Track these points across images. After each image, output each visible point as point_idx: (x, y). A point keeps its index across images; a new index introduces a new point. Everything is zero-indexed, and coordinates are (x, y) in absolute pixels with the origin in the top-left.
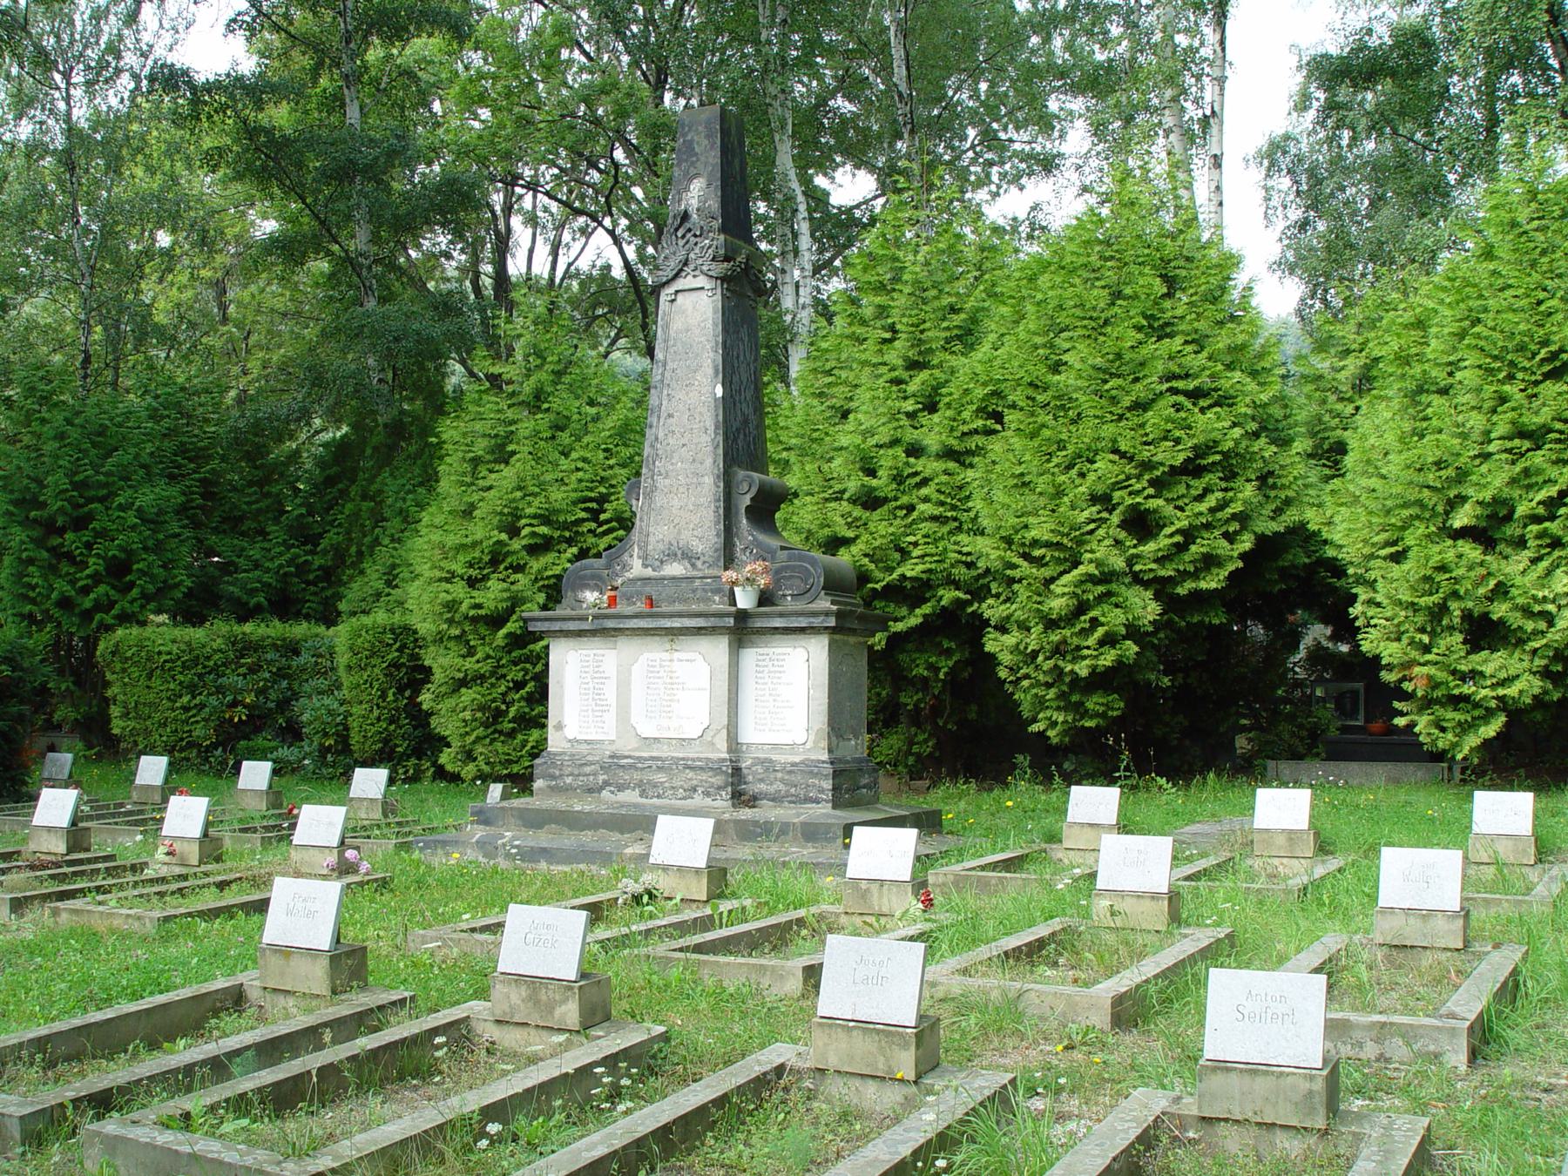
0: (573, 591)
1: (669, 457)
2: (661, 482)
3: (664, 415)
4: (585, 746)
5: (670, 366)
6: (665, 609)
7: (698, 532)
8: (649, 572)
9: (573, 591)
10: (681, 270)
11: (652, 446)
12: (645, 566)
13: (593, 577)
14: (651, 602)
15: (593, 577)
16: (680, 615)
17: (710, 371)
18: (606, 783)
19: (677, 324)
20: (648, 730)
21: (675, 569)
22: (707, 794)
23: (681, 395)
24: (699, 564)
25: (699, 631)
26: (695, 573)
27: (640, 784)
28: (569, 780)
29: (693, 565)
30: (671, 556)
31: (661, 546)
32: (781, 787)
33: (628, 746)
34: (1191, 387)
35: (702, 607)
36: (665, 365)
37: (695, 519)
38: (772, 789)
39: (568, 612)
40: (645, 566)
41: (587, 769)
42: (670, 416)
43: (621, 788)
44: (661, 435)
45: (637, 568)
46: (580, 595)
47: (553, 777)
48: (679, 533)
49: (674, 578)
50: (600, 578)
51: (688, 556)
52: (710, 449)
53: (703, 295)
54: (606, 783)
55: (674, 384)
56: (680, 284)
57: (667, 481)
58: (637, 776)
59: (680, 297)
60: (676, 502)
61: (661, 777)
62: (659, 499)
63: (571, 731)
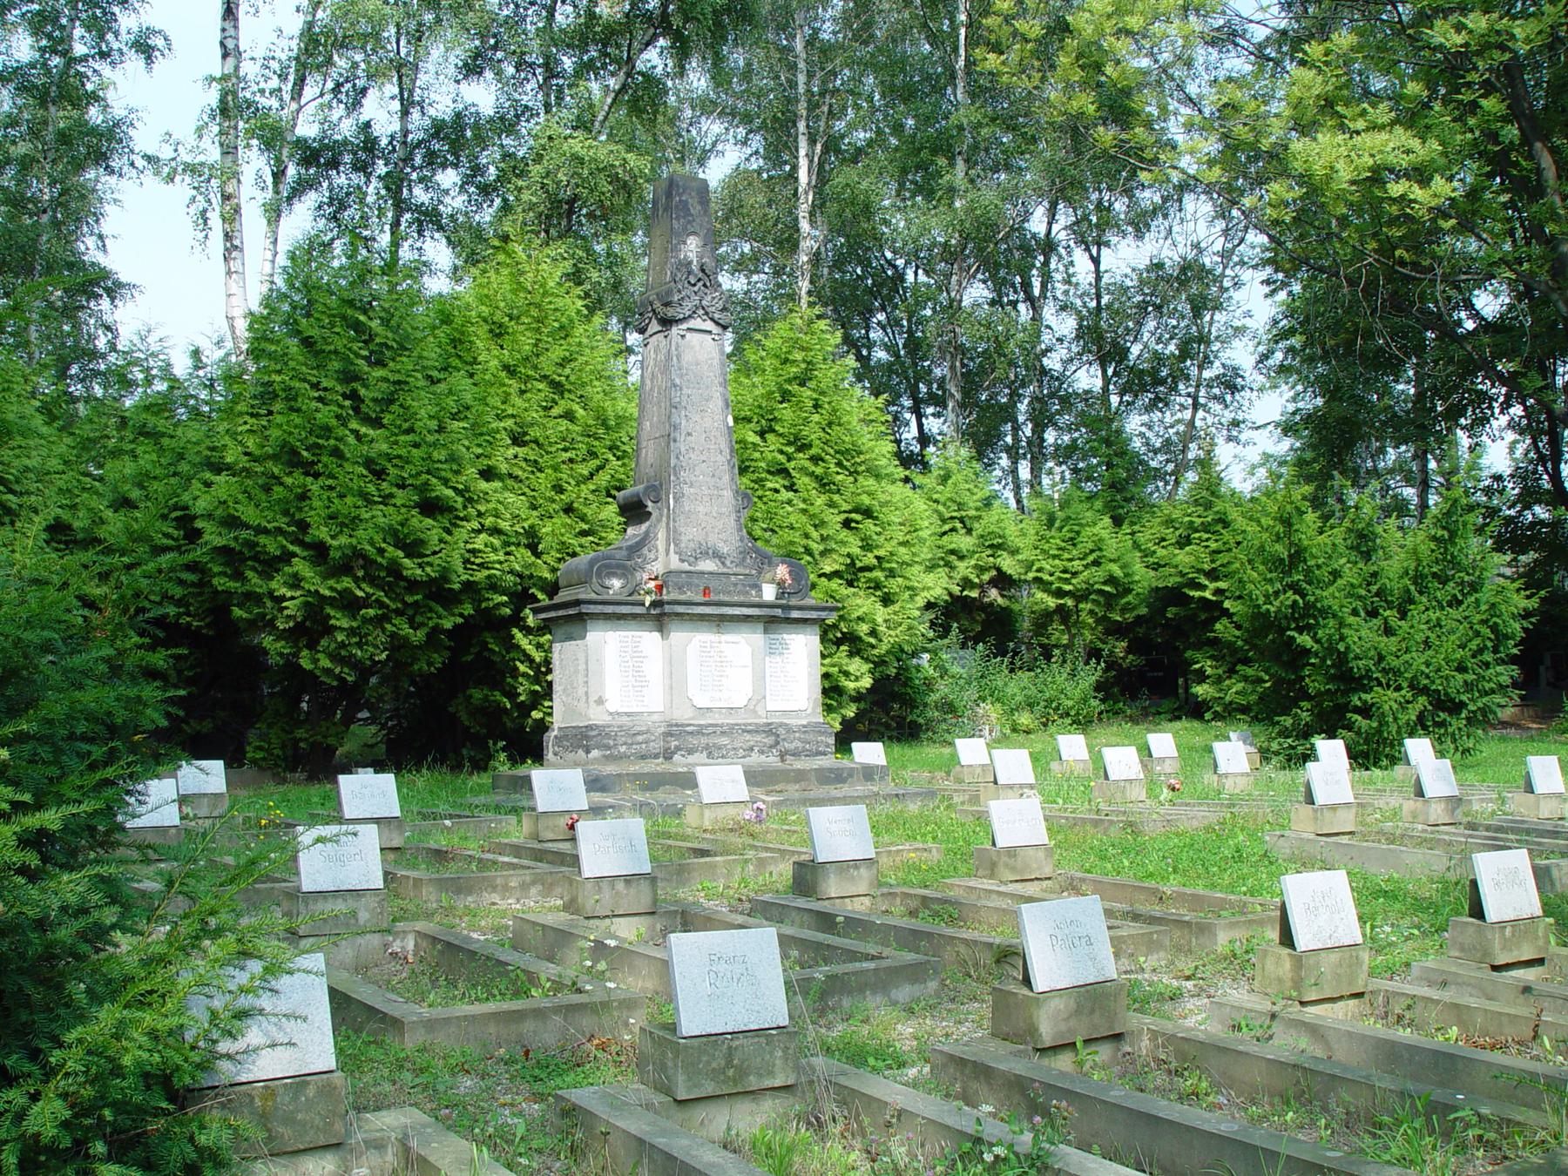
4: (625, 718)
5: (685, 391)
8: (686, 566)
13: (618, 566)
14: (706, 591)
15: (618, 566)
17: (720, 403)
18: (678, 748)
19: (687, 358)
20: (701, 702)
21: (708, 565)
22: (762, 752)
25: (747, 619)
27: (707, 747)
28: (623, 749)
31: (692, 545)
32: (800, 745)
33: (683, 715)
35: (742, 599)
38: (792, 746)
39: (593, 596)
40: (682, 561)
41: (640, 738)
42: (689, 434)
43: (691, 752)
46: (607, 582)
47: (609, 748)
50: (624, 567)
52: (726, 467)
53: (708, 337)
54: (678, 748)
56: (692, 324)
58: (704, 740)
60: (701, 509)
61: (724, 741)
63: (612, 706)
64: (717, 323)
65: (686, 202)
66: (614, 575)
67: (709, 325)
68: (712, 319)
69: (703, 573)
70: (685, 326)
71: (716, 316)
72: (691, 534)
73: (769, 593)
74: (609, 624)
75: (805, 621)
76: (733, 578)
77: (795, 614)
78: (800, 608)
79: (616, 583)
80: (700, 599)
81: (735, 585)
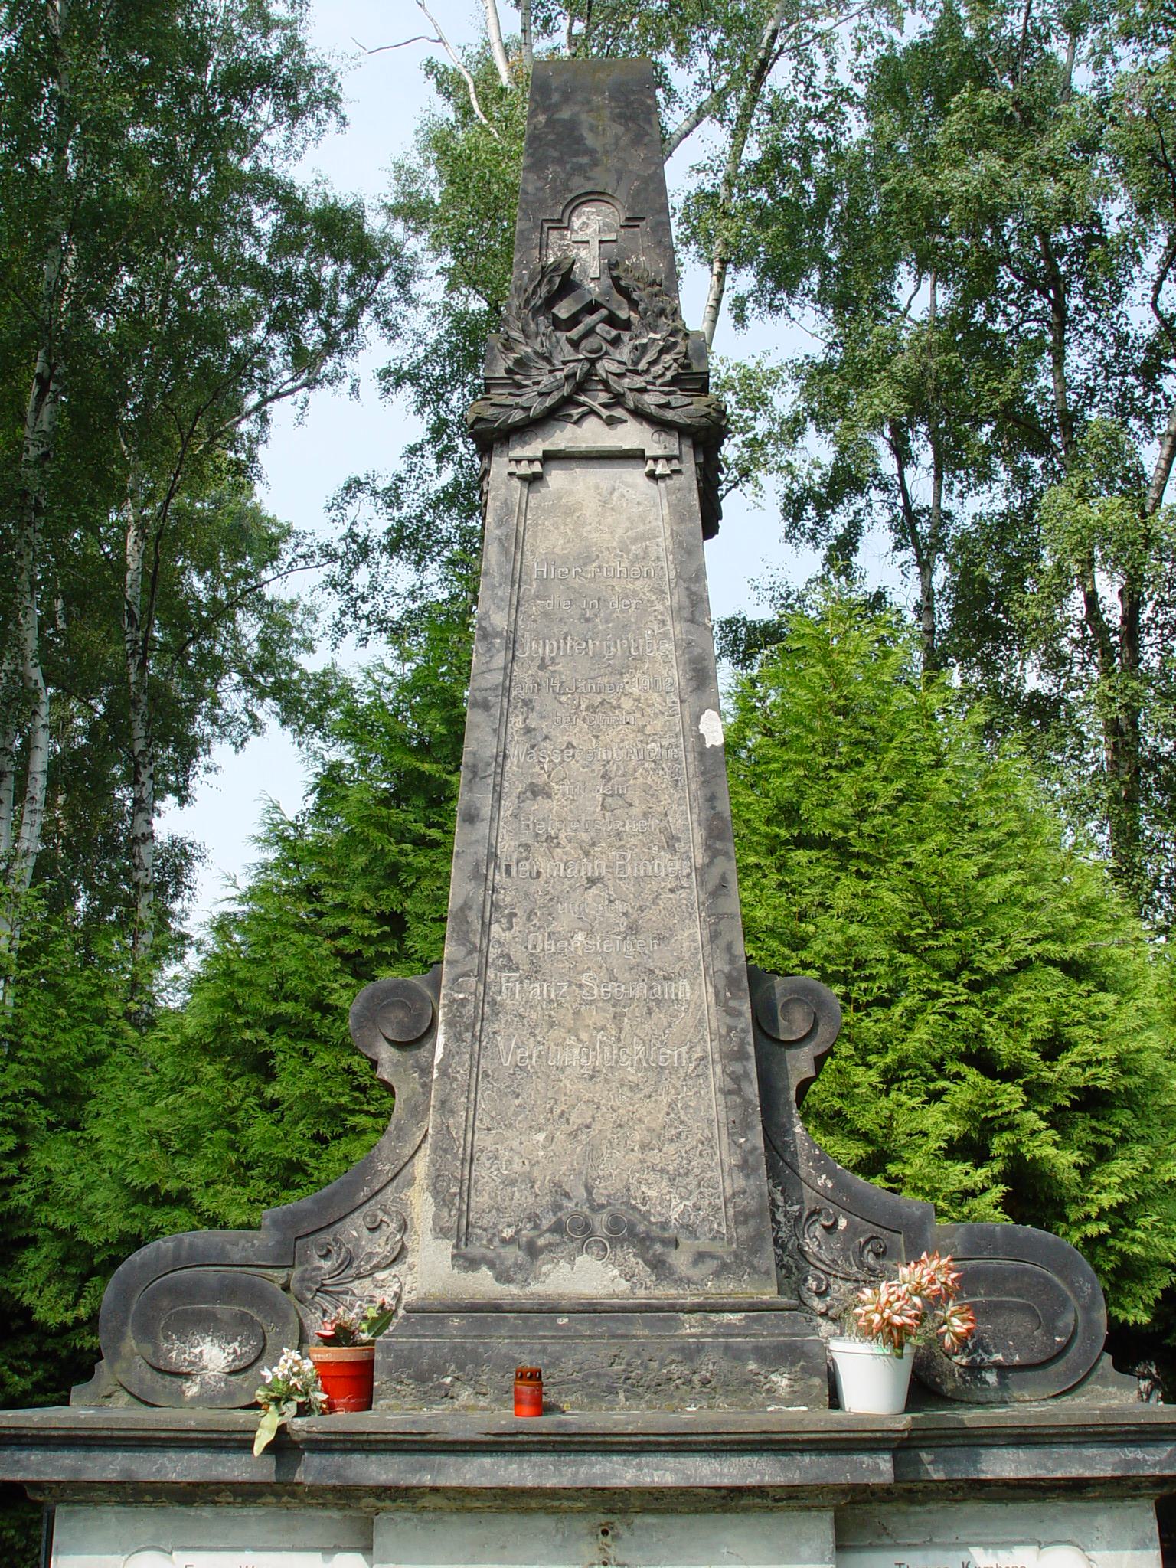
0: (147, 1332)
1: (542, 912)
2: (509, 989)
3: (513, 787)
5: (530, 648)
6: (576, 1415)
7: (668, 1155)
8: (483, 1284)
9: (147, 1332)
10: (568, 401)
11: (478, 876)
12: (467, 1262)
15: (229, 1291)
16: (680, 1445)
19: (548, 541)
21: (588, 1276)
23: (577, 734)
24: (680, 1260)
25: (730, 1500)
26: (665, 1292)
29: (658, 1266)
30: (575, 1232)
31: (522, 1198)
34: (1066, 956)
36: (512, 643)
37: (653, 1113)
39: (121, 1412)
40: (467, 1262)
42: (536, 791)
44: (507, 846)
45: (429, 1269)
46: (177, 1353)
48: (592, 1153)
49: (591, 1309)
50: (256, 1295)
51: (630, 1233)
53: (634, 476)
55: (545, 701)
56: (563, 437)
57: (537, 990)
59: (557, 478)
60: (572, 1056)
62: (507, 1046)
64: (661, 425)
65: (572, 125)
66: (205, 1323)
67: (632, 435)
68: (639, 414)
69: (549, 1309)
70: (536, 447)
71: (651, 400)
72: (521, 1160)
73: (869, 1384)
74: (147, 1521)
75: (1075, 1489)
76: (690, 1326)
77: (1005, 1465)
78: (1024, 1437)
79: (213, 1356)
80: (505, 1418)
81: (690, 1353)
